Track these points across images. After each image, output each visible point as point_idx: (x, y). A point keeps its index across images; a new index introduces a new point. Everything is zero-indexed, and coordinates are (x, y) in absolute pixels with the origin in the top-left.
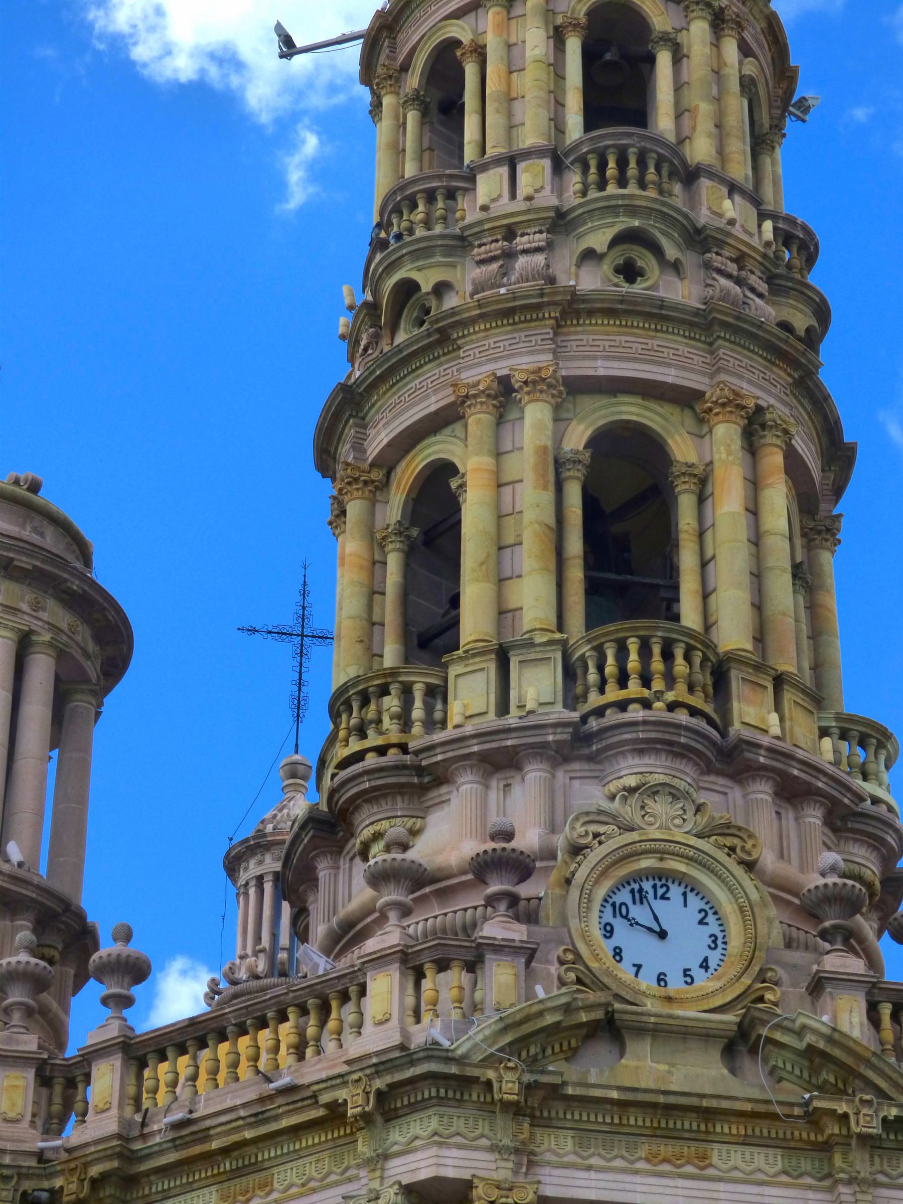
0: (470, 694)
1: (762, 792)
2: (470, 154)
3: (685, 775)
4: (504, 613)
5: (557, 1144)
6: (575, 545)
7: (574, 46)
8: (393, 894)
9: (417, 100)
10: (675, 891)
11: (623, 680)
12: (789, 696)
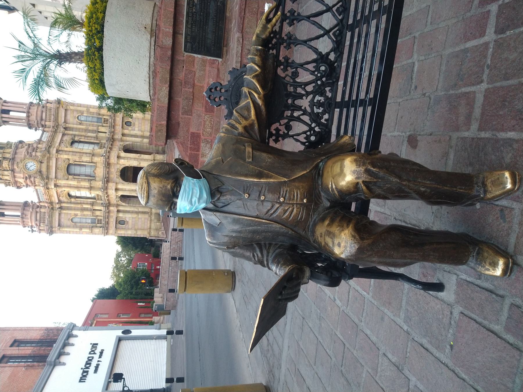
1: (16, 156)
3: (16, 163)
5: (50, 176)
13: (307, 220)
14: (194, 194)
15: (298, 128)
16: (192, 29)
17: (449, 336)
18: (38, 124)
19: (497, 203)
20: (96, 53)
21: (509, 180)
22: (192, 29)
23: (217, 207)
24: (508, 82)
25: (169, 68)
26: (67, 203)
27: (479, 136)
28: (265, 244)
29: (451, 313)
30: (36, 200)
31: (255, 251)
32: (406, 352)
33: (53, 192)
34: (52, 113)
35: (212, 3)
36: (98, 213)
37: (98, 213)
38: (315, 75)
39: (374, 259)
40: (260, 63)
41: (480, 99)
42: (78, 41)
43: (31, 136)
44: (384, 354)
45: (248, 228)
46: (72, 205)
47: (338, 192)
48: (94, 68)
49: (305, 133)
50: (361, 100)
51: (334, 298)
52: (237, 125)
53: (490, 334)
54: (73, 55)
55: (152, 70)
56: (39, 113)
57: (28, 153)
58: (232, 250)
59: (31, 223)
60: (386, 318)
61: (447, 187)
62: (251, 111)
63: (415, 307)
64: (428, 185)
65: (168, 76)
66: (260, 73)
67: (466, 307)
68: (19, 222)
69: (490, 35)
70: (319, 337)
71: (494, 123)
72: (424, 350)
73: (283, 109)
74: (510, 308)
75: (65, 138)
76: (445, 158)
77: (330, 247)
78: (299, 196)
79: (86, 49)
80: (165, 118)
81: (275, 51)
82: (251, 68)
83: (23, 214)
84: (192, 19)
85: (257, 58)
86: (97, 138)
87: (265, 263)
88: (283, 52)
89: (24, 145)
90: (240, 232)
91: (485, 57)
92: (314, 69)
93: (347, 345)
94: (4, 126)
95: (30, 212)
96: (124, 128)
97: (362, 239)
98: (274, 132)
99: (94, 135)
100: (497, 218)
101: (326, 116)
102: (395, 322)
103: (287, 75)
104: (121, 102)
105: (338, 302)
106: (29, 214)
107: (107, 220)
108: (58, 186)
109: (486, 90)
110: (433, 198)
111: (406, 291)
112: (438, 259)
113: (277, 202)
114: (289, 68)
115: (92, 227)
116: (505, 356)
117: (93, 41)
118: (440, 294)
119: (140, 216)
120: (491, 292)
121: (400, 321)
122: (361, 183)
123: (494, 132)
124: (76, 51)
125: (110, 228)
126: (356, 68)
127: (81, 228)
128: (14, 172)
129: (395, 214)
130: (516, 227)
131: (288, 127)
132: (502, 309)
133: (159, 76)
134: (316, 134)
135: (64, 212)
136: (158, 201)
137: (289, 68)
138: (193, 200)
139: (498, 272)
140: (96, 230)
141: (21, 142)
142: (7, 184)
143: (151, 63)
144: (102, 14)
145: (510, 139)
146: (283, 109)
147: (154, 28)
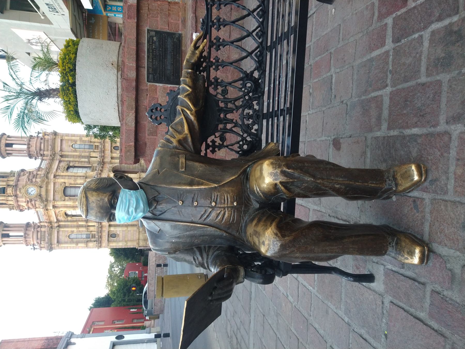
1: (19, 183)
3: (18, 189)
5: (49, 199)
13: (239, 222)
14: (131, 205)
15: (231, 138)
16: (153, 63)
17: (383, 325)
18: (37, 153)
19: (410, 194)
20: (70, 88)
21: (415, 173)
22: (153, 63)
23: (156, 215)
24: (408, 84)
25: (134, 96)
26: (65, 221)
27: (389, 135)
28: (205, 247)
29: (383, 303)
30: (37, 221)
31: (196, 255)
32: (349, 343)
33: (52, 212)
34: (50, 143)
35: (169, 40)
36: (92, 229)
37: (92, 229)
38: (242, 91)
39: (297, 255)
40: (191, 84)
41: (386, 101)
42: (54, 80)
43: (31, 165)
44: (331, 346)
45: (186, 233)
46: (69, 223)
47: (262, 193)
48: (69, 101)
49: (238, 143)
50: (282, 110)
51: (287, 294)
52: (172, 139)
53: (417, 321)
54: (51, 92)
55: (120, 99)
56: (38, 144)
57: (29, 179)
58: (173, 255)
59: (33, 241)
60: (330, 311)
61: (358, 182)
62: (184, 126)
63: (353, 298)
64: (341, 182)
65: (134, 104)
66: (191, 92)
67: (394, 296)
68: (22, 242)
69: (389, 45)
70: (277, 333)
71: (400, 121)
72: (363, 340)
73: (217, 123)
74: (432, 294)
75: (62, 164)
76: (363, 157)
77: (257, 246)
78: (229, 199)
79: (61, 86)
80: (133, 140)
81: (205, 74)
82: (183, 88)
83: (25, 234)
84: (153, 54)
85: (188, 80)
87: (206, 265)
88: (213, 73)
89: (26, 173)
90: (179, 237)
91: (387, 63)
92: (241, 86)
93: (301, 340)
94: (7, 158)
95: (31, 232)
96: (113, 152)
97: (283, 236)
98: (211, 144)
99: (86, 160)
100: (411, 208)
101: (256, 127)
102: (337, 314)
103: (218, 93)
104: (105, 129)
105: (290, 298)
106: (31, 233)
107: (100, 234)
108: (56, 207)
109: (391, 93)
110: (351, 194)
111: (344, 284)
112: (357, 251)
113: (209, 207)
114: (219, 87)
115: (87, 242)
116: (432, 343)
117: (67, 78)
118: (372, 285)
119: (129, 228)
120: (414, 280)
121: (341, 313)
122: (279, 184)
123: (401, 130)
124: (54, 88)
125: (103, 241)
126: (274, 82)
127: (77, 243)
128: (17, 197)
129: (329, 211)
130: (428, 216)
131: (223, 139)
132: (425, 296)
133: (126, 104)
134: (248, 143)
135: (62, 229)
136: (96, 213)
137: (219, 87)
138: (130, 210)
139: (416, 260)
140: (91, 244)
141: (23, 170)
142: (11, 208)
143: (119, 94)
144: (74, 55)
145: (414, 135)
146: (217, 123)
147: (120, 64)
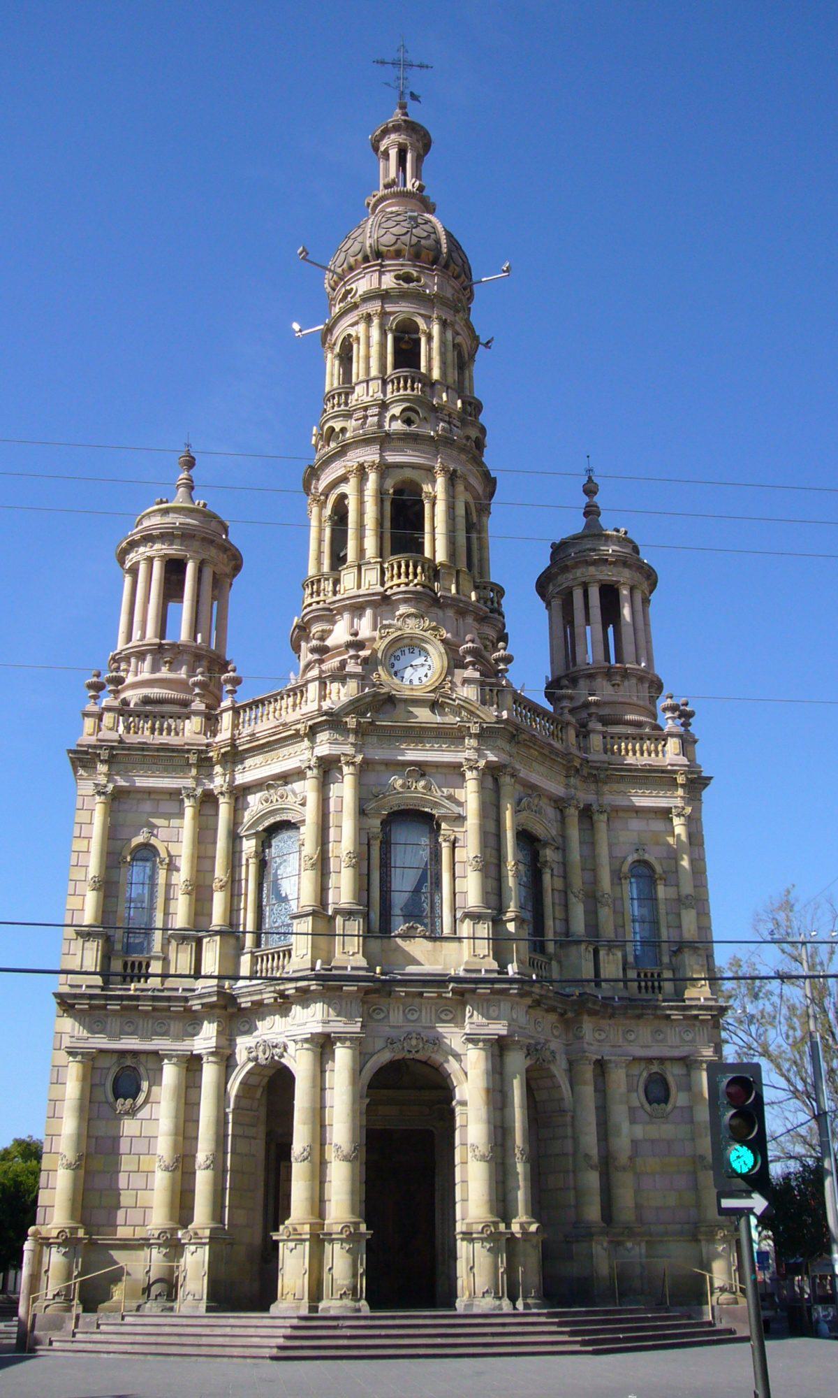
0: (348, 579)
2: (354, 380)
4: (361, 551)
6: (388, 524)
7: (390, 337)
8: (316, 657)
9: (339, 356)
10: (416, 650)
11: (399, 577)
12: (461, 576)
26: (235, 822)
59: (135, 685)
86: (567, 940)
